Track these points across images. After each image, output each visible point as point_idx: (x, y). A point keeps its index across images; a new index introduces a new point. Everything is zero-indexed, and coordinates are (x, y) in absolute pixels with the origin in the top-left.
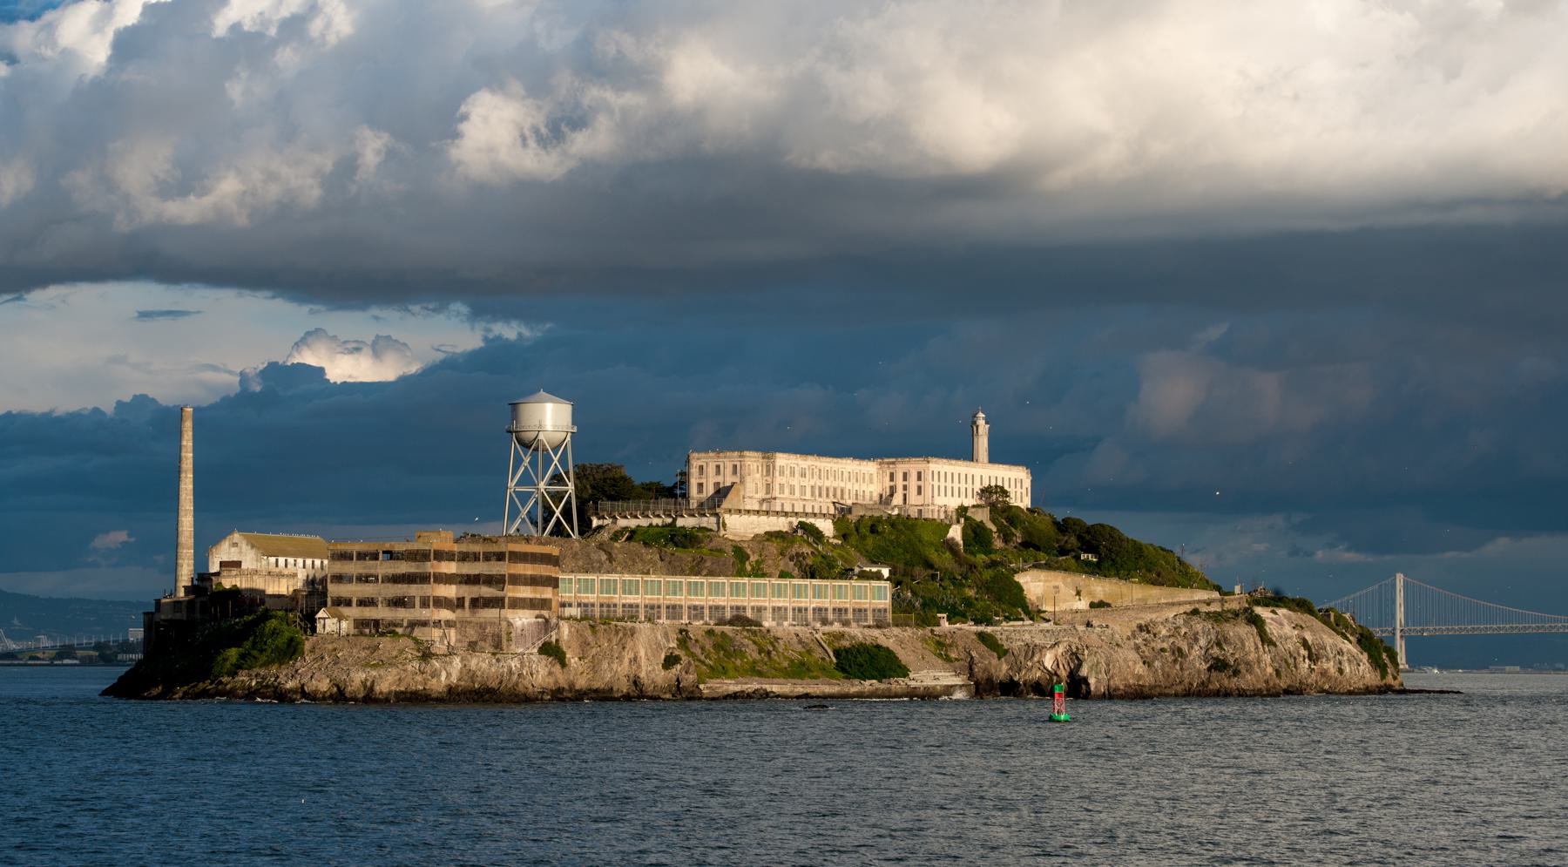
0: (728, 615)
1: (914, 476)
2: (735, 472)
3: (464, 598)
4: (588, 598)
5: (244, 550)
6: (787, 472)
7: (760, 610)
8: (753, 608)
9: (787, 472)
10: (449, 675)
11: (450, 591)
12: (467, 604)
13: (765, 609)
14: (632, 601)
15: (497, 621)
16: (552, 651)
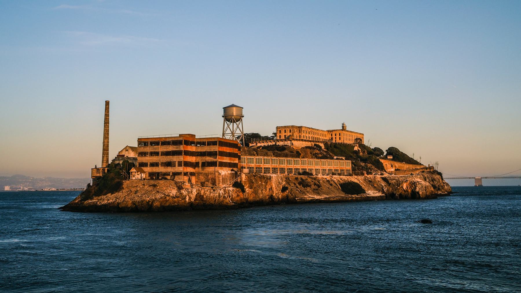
0: (301, 171)
1: (338, 134)
2: (290, 132)
3: (199, 162)
4: (251, 165)
5: (130, 152)
6: (305, 132)
7: (311, 170)
8: (309, 169)
9: (305, 132)
10: (190, 198)
11: (192, 159)
12: (200, 165)
13: (313, 169)
14: (267, 167)
15: (214, 173)
16: (238, 185)
